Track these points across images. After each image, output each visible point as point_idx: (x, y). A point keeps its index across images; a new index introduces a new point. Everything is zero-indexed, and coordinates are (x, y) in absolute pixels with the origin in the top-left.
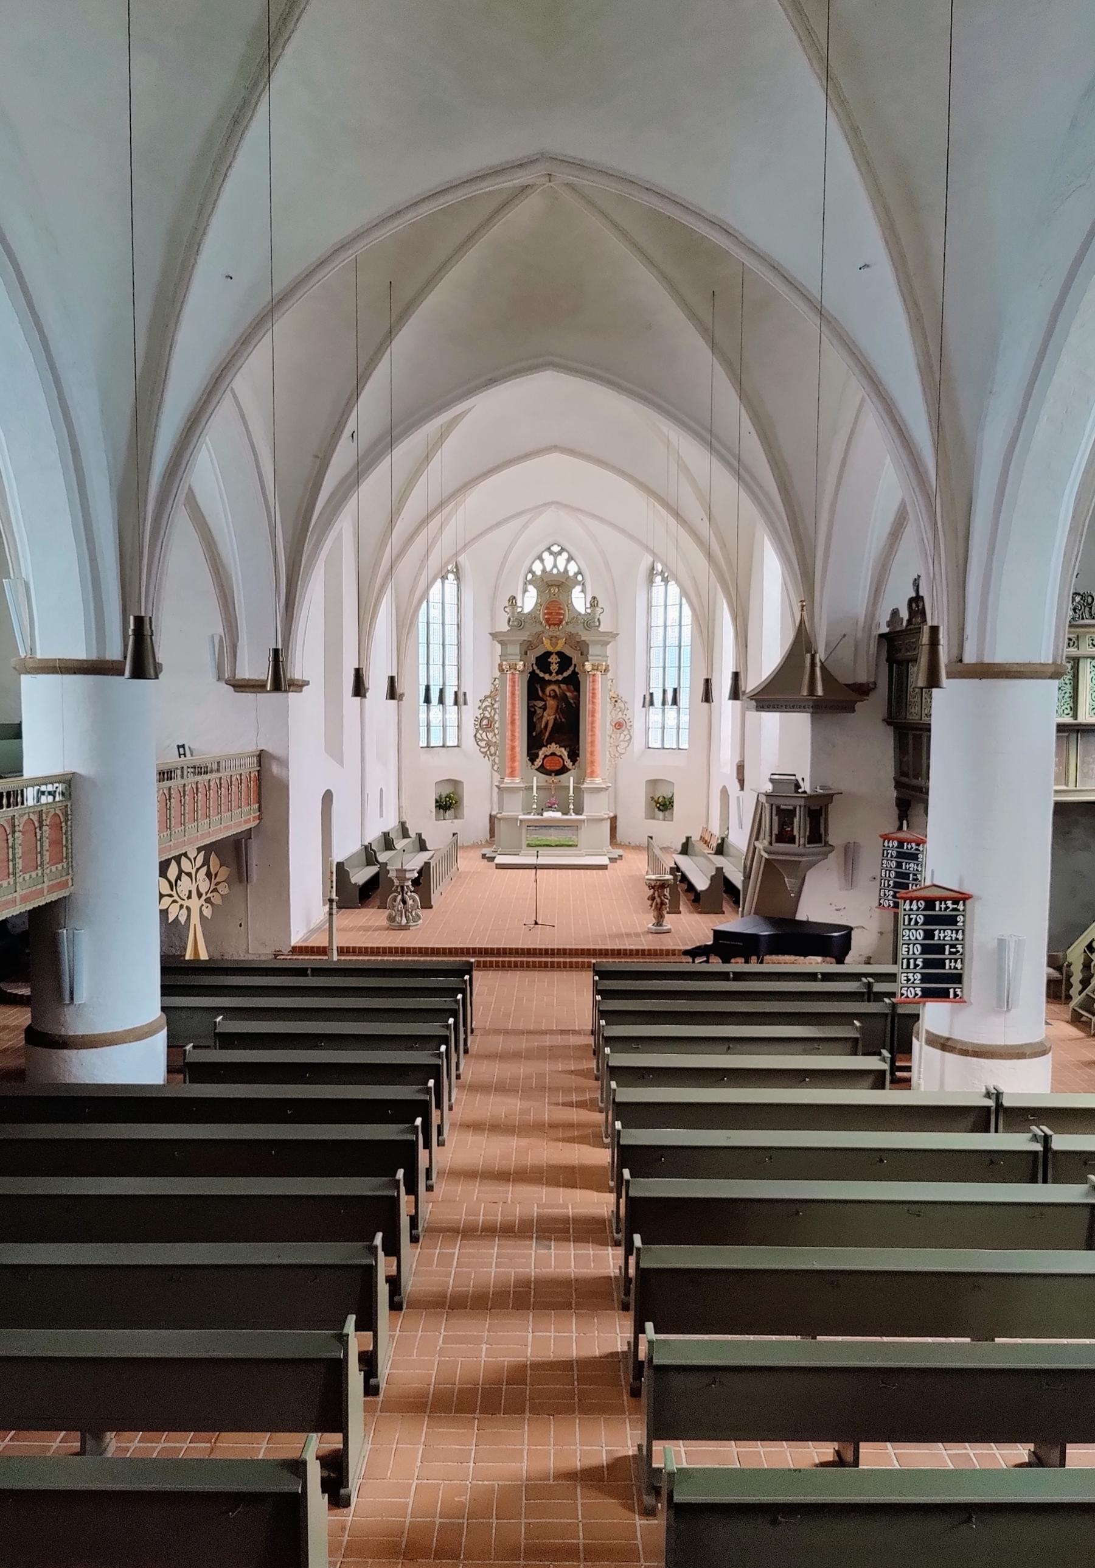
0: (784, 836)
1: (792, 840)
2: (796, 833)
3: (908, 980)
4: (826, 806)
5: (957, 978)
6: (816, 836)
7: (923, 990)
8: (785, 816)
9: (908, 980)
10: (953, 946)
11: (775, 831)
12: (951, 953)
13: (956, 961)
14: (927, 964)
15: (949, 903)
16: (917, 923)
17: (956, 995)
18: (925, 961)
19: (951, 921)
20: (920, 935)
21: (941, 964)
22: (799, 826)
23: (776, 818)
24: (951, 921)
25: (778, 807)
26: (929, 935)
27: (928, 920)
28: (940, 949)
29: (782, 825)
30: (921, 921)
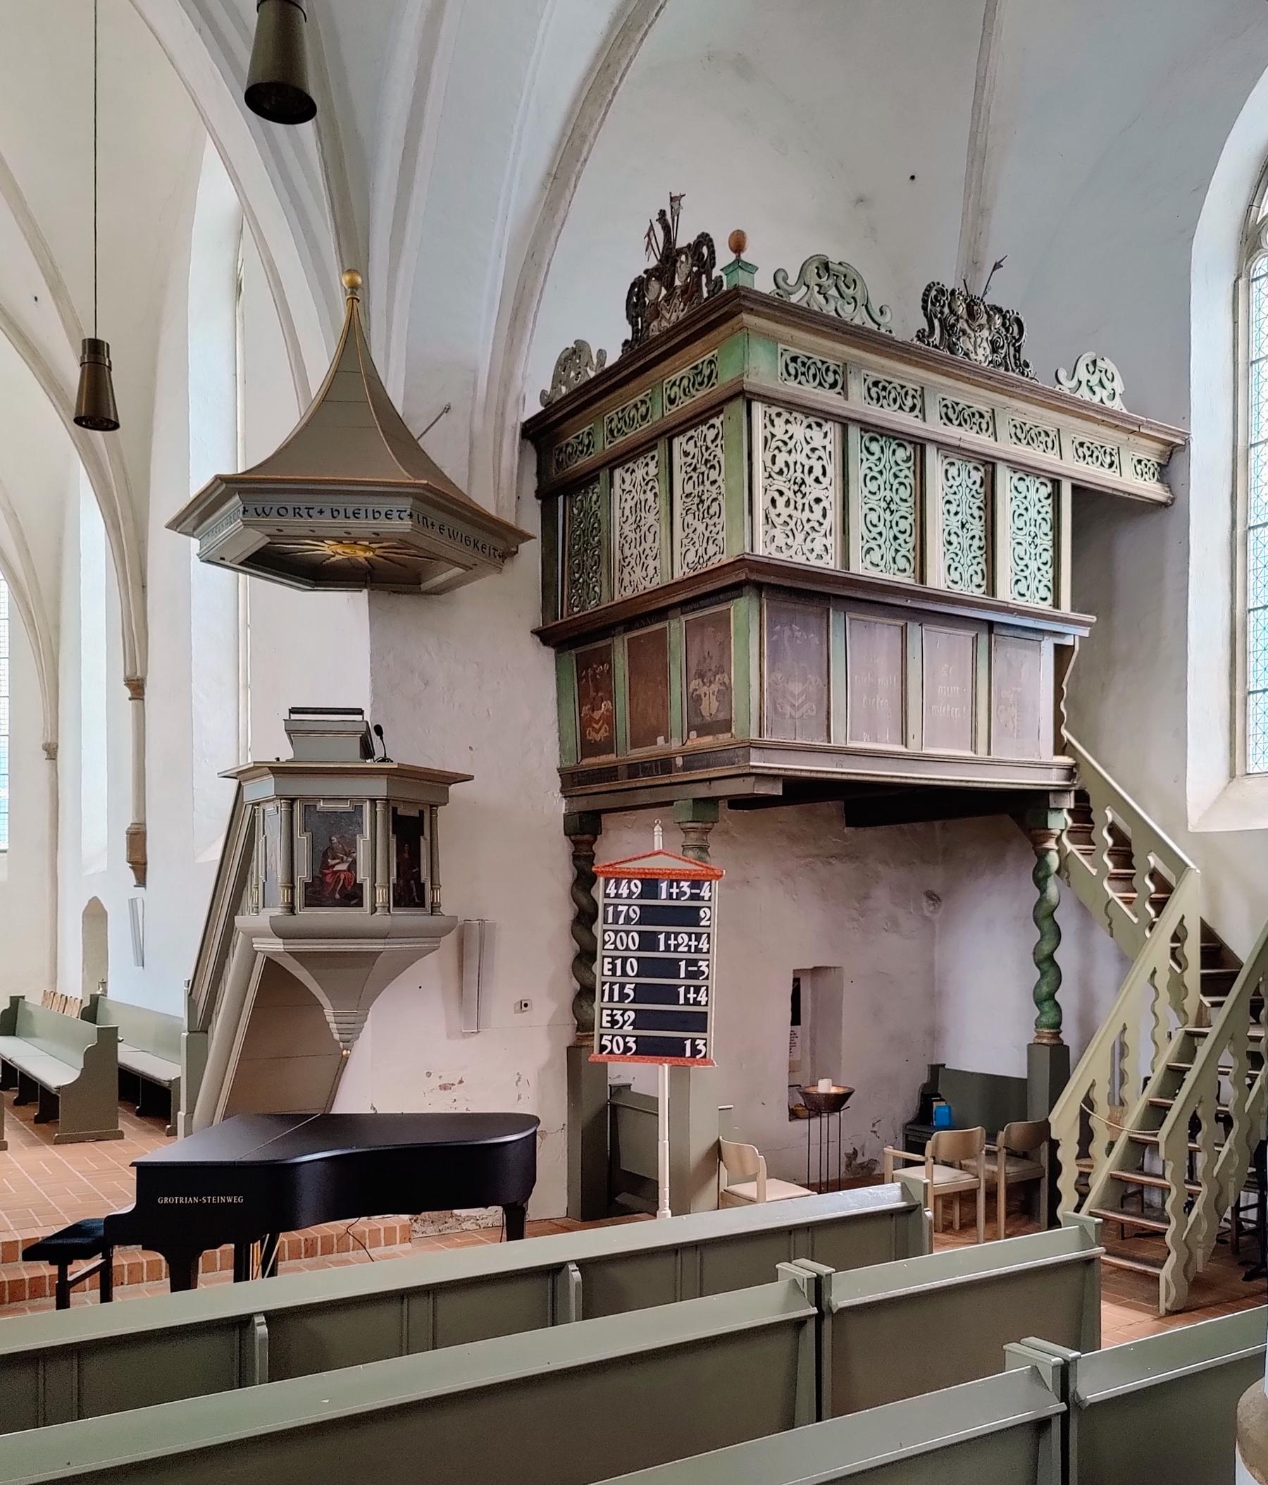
0: (329, 886)
1: (352, 896)
2: (363, 876)
3: (613, 1022)
4: (433, 807)
5: (698, 1022)
6: (410, 890)
7: (638, 1040)
8: (327, 835)
9: (613, 1022)
10: (690, 962)
11: (303, 873)
12: (690, 975)
13: (697, 991)
14: (643, 993)
15: (685, 885)
16: (628, 920)
17: (695, 1051)
18: (637, 988)
19: (689, 916)
20: (634, 940)
21: (670, 994)
22: (370, 856)
23: (303, 842)
24: (689, 916)
25: (309, 808)
26: (648, 941)
27: (649, 915)
28: (670, 968)
29: (322, 857)
30: (635, 917)
